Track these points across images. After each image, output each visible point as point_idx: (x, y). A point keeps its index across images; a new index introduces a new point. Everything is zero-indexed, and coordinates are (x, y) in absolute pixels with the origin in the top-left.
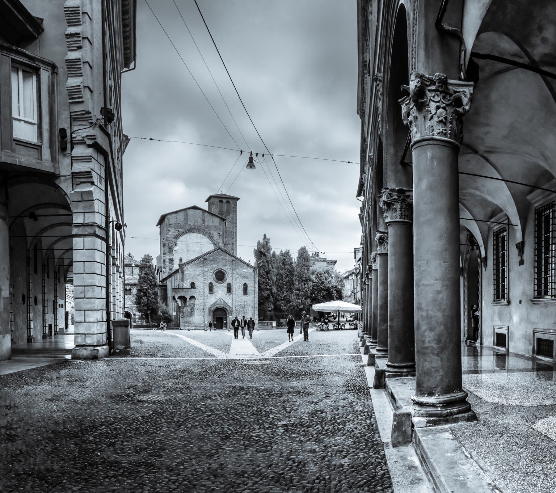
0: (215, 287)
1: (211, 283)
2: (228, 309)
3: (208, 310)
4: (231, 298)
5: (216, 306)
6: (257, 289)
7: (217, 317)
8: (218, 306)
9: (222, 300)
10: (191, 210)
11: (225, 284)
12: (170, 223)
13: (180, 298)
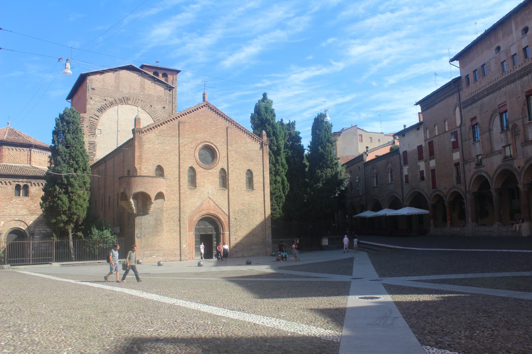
0: (198, 177)
1: (192, 169)
2: (223, 219)
3: (187, 222)
4: (226, 197)
5: (200, 214)
6: (267, 181)
7: (201, 235)
8: (204, 212)
9: (211, 201)
10: (125, 71)
11: (216, 171)
12: (94, 87)
13: (136, 196)
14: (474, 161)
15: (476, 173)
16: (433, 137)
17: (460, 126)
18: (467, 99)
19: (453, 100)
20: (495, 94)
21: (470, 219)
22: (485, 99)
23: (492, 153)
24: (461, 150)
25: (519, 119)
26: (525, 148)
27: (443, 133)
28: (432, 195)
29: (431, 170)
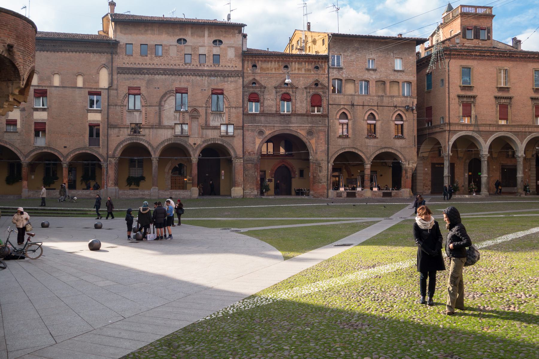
14: (128, 128)
15: (129, 139)
16: (48, 87)
17: (108, 89)
18: (124, 66)
19: (104, 59)
20: (173, 77)
21: (111, 182)
22: (157, 77)
23: (160, 126)
24: (106, 112)
25: (202, 107)
26: (204, 131)
27: (72, 87)
28: (33, 151)
29: (35, 122)
